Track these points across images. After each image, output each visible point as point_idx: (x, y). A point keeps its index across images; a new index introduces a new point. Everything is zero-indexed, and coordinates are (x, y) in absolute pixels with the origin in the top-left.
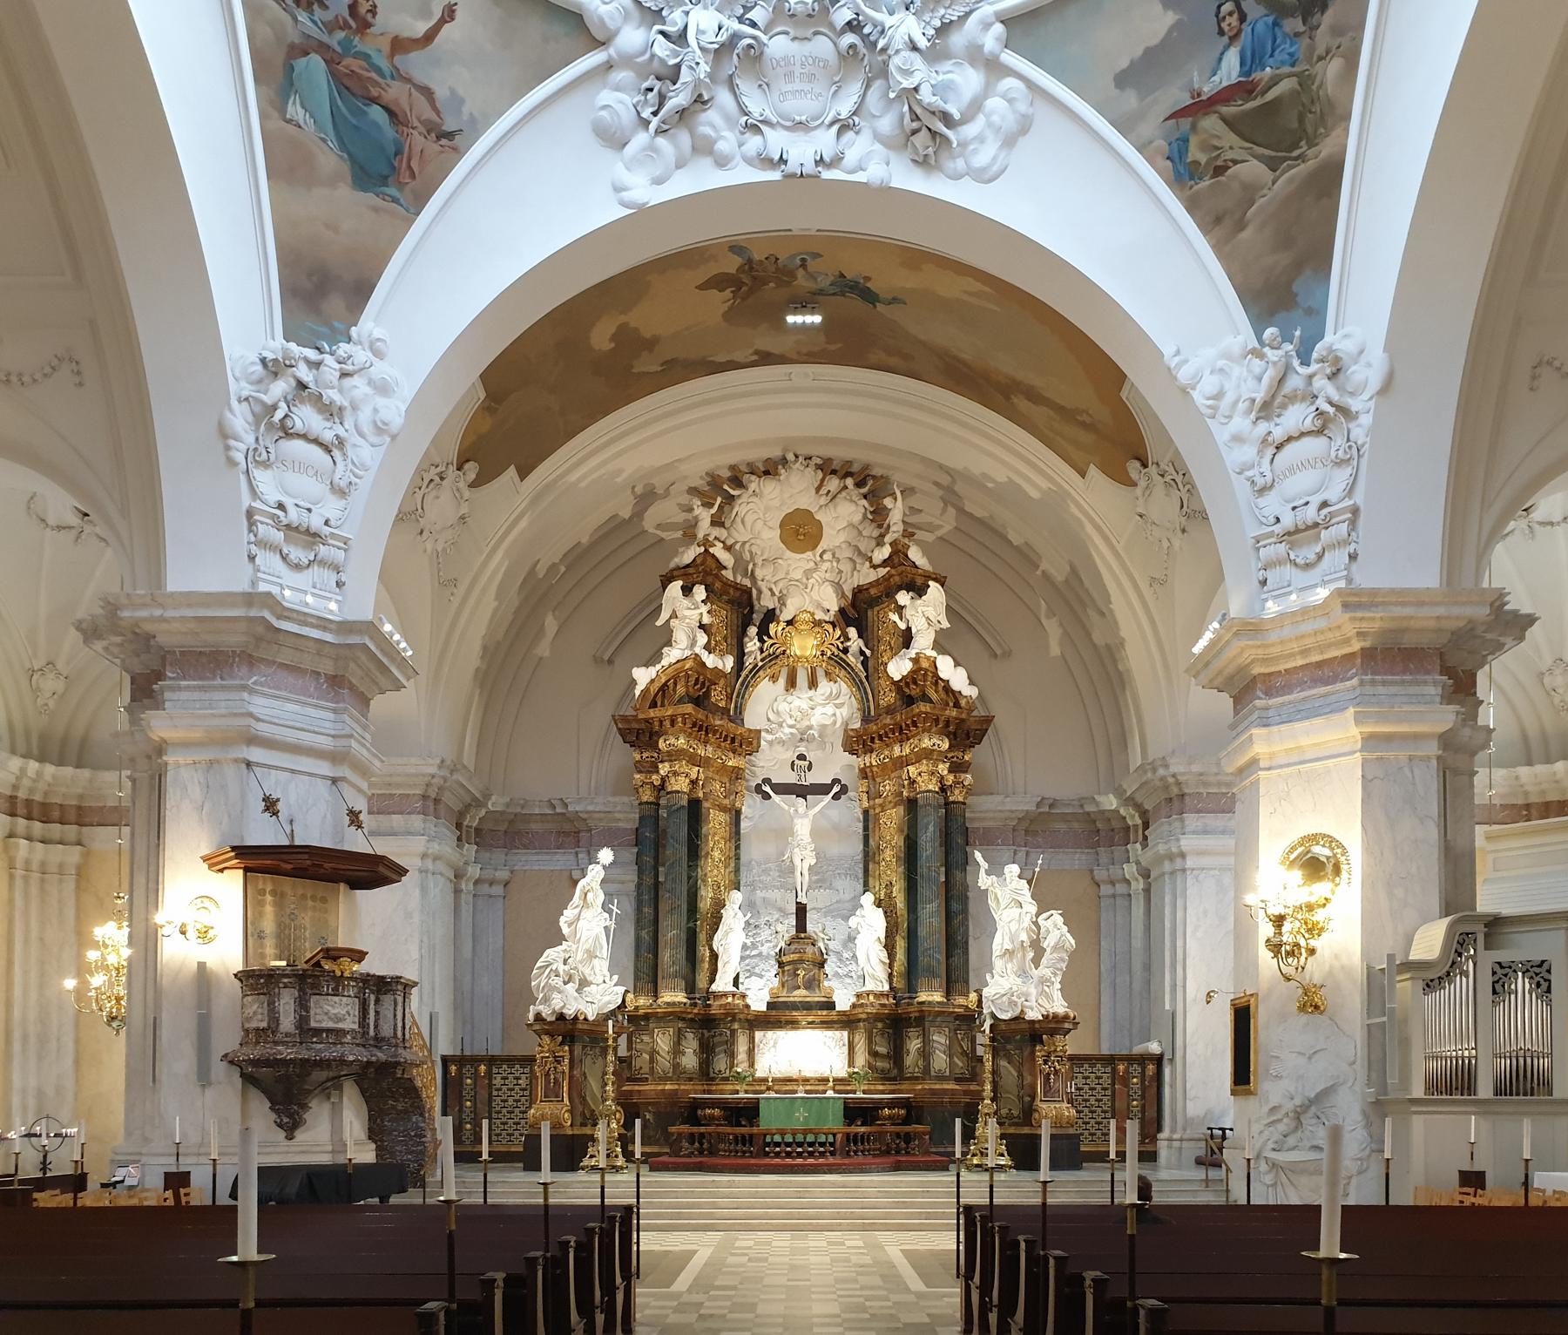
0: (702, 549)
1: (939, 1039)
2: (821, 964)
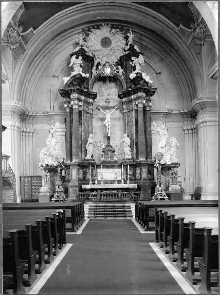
0: (80, 47)
1: (145, 170)
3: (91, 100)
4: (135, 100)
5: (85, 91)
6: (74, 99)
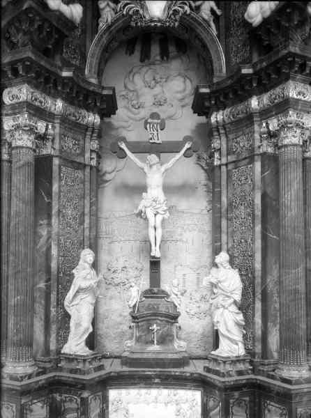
2: (174, 318)
3: (93, 119)
4: (265, 113)
5: (65, 74)
6: (17, 108)
